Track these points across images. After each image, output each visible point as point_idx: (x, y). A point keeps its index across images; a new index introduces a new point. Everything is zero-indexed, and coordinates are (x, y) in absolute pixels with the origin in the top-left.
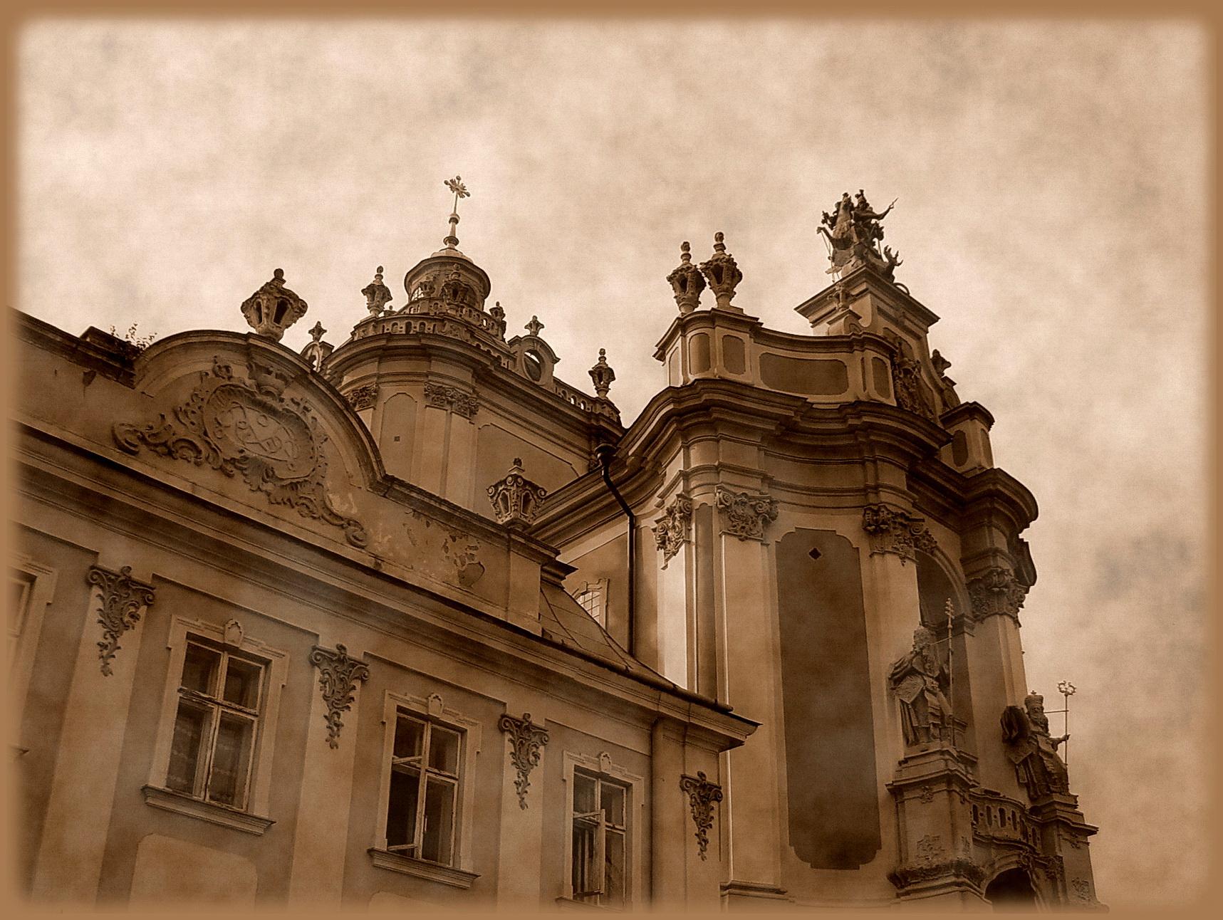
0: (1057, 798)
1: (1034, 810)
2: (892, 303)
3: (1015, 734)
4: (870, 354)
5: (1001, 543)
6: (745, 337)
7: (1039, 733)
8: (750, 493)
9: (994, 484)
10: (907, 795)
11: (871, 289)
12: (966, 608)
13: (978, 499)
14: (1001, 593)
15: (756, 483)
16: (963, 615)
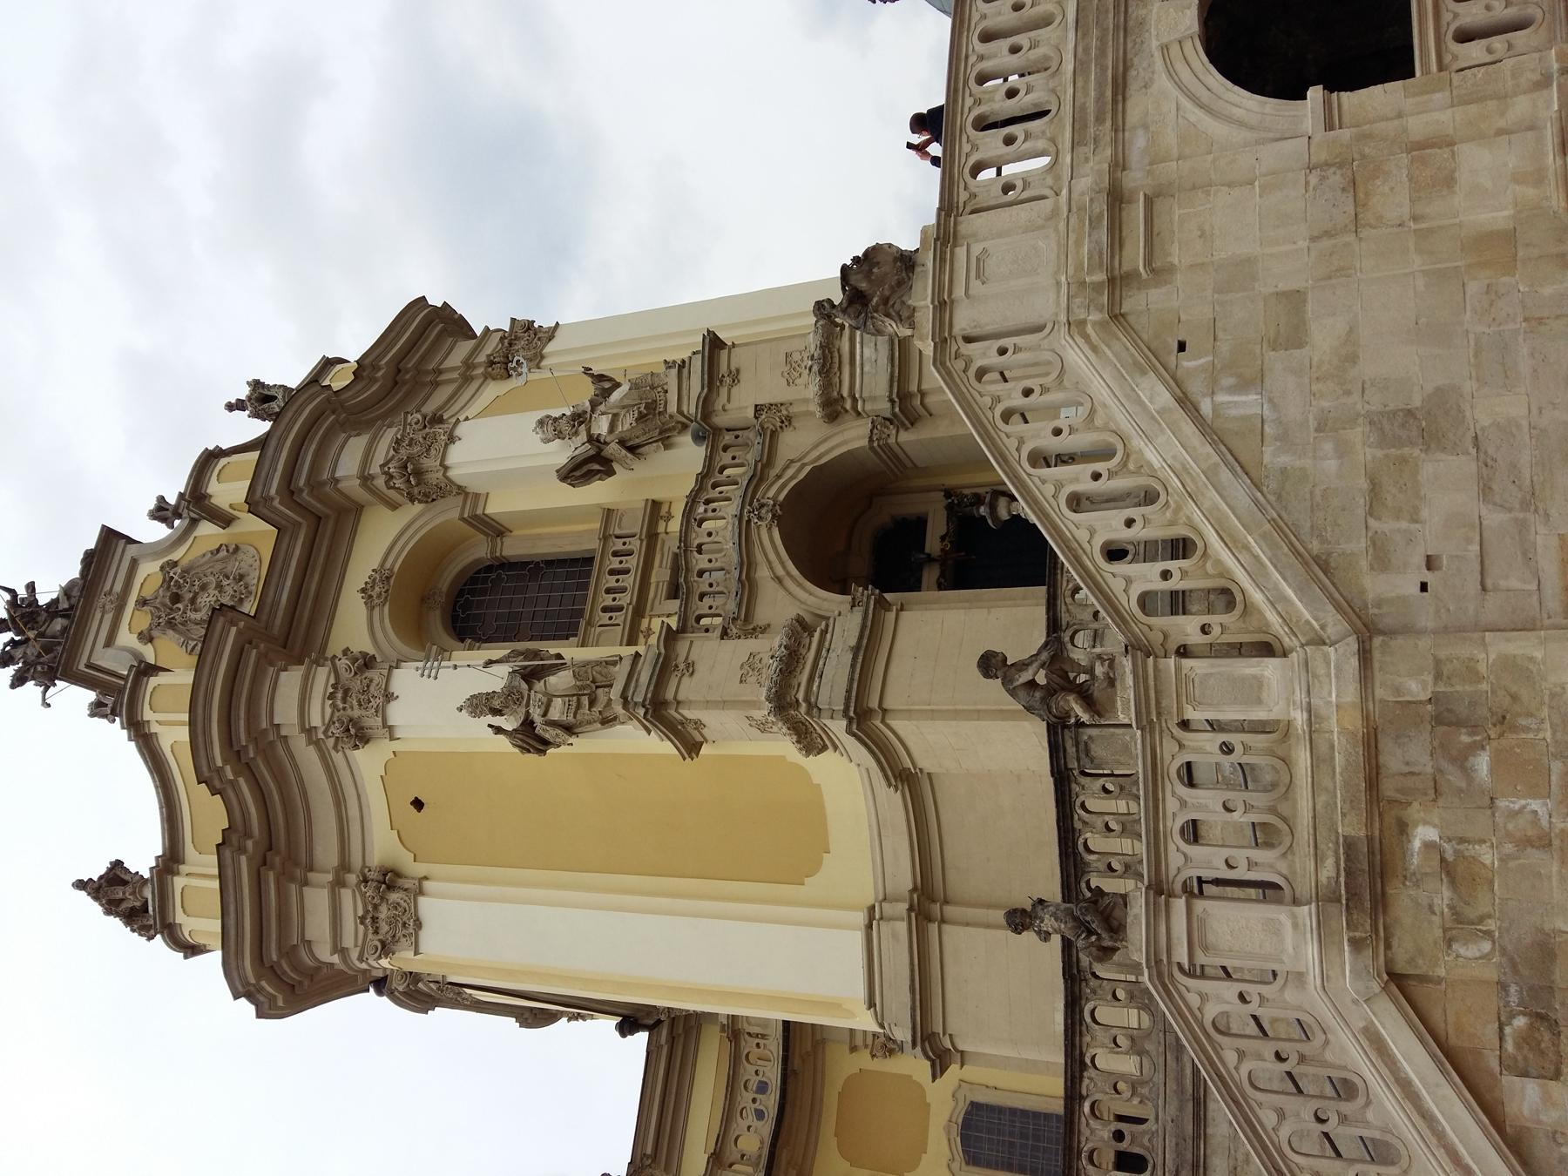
0: (672, 408)
1: (698, 438)
2: (98, 615)
3: (597, 467)
4: (148, 715)
5: (350, 460)
6: (179, 882)
7: (588, 430)
8: (360, 913)
9: (272, 499)
10: (699, 738)
11: (84, 660)
12: (448, 513)
13: (302, 508)
14: (419, 473)
15: (346, 895)
16: (462, 519)
